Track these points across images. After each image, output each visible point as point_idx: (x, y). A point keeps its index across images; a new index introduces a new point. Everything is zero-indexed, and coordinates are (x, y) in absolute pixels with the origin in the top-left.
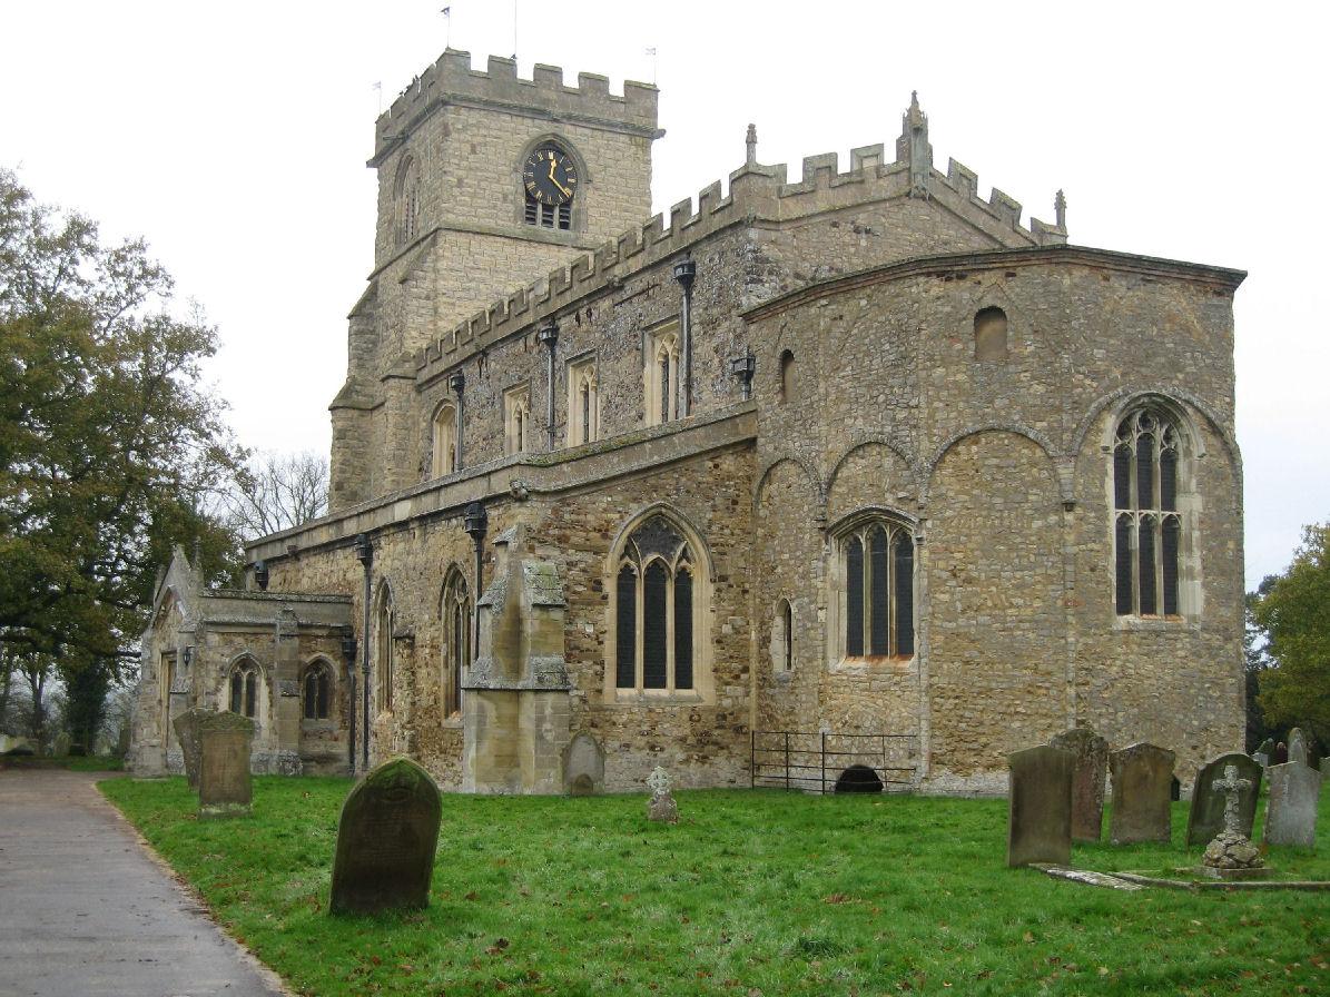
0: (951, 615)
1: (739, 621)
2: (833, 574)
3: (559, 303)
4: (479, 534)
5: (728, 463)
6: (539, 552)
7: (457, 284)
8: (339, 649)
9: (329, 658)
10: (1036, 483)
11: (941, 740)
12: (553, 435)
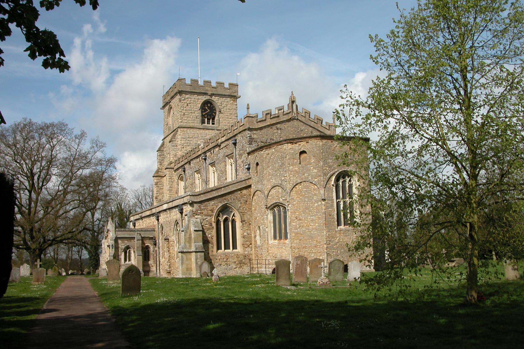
0: (296, 228)
1: (249, 232)
3: (207, 149)
4: (182, 213)
5: (245, 192)
6: (196, 217)
7: (184, 142)
8: (152, 243)
9: (150, 245)
10: (315, 195)
12: (207, 183)
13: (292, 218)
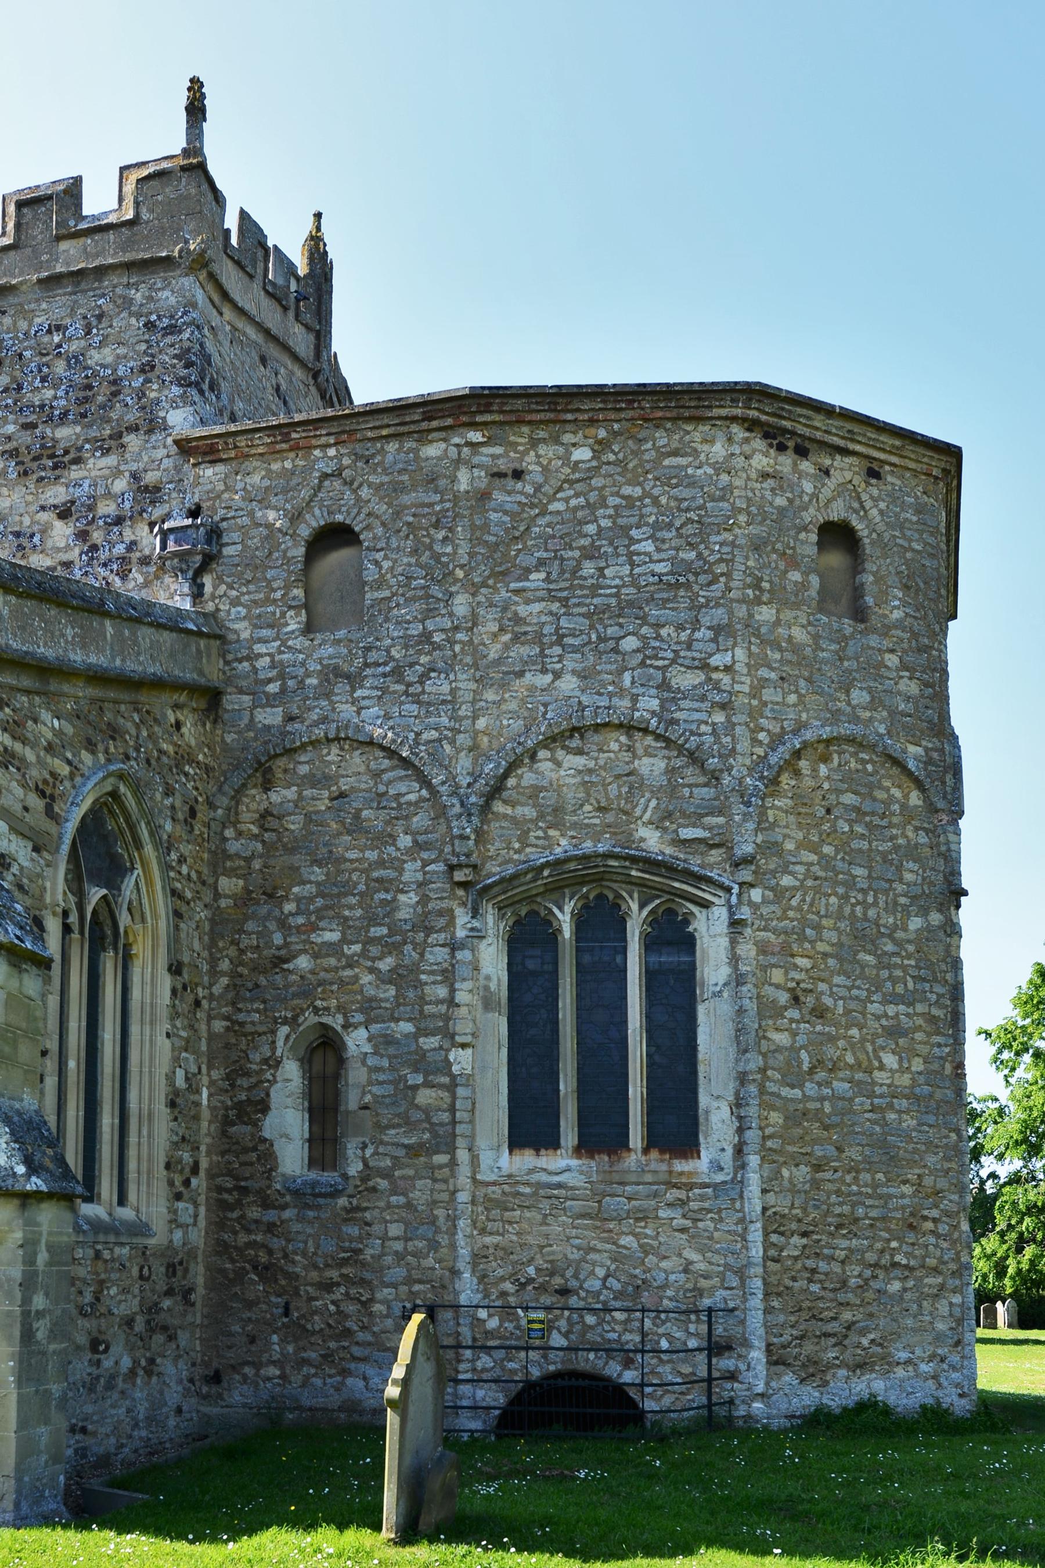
2: (488, 978)
11: (782, 1318)
13: (769, 991)
